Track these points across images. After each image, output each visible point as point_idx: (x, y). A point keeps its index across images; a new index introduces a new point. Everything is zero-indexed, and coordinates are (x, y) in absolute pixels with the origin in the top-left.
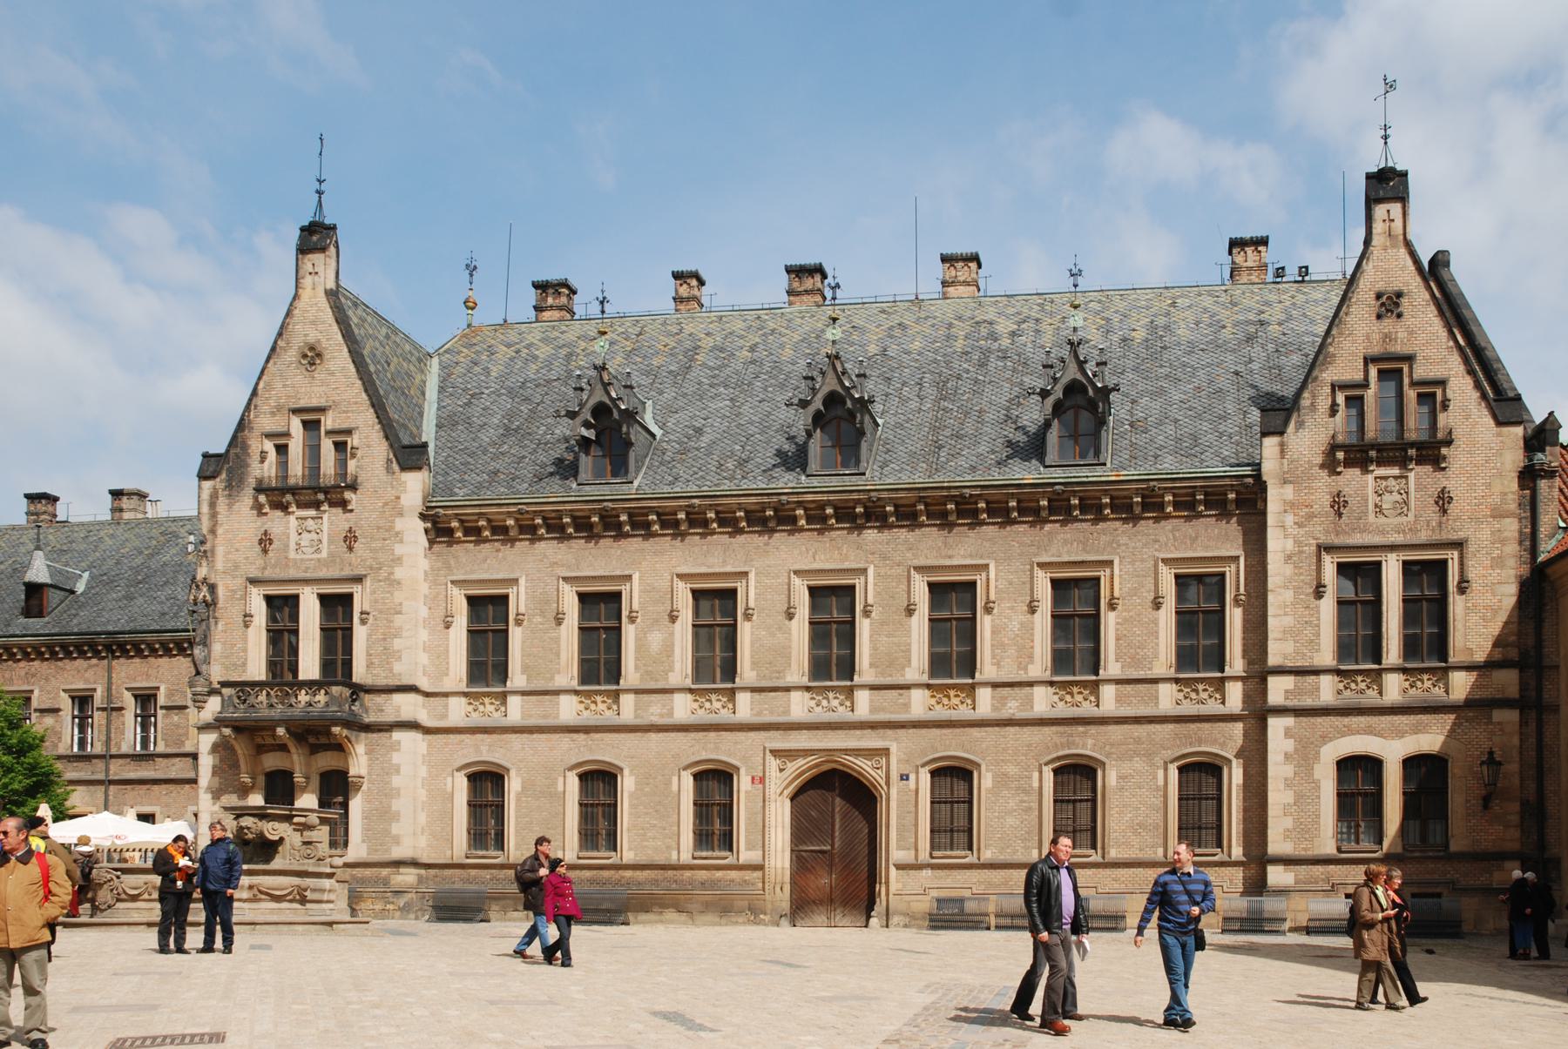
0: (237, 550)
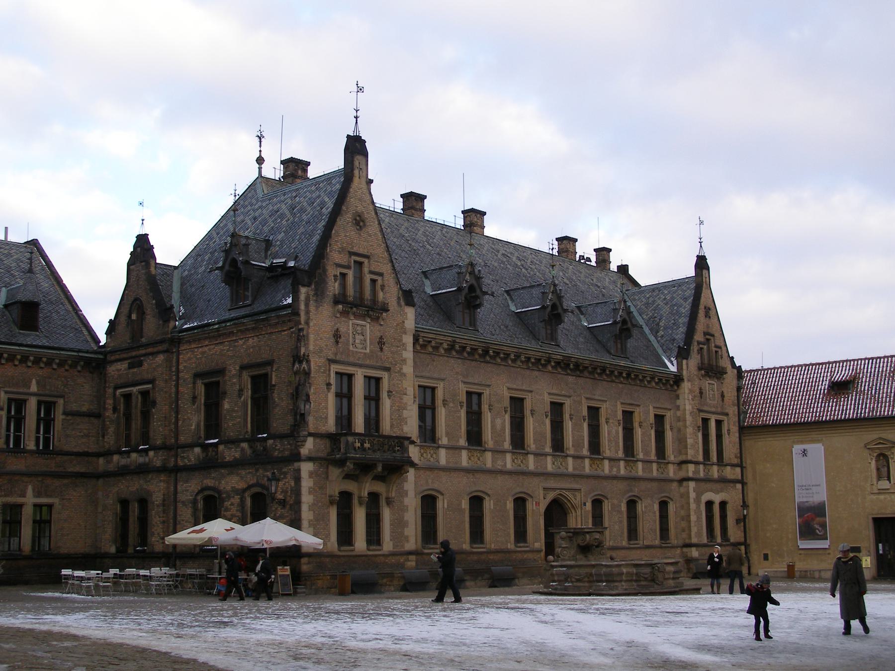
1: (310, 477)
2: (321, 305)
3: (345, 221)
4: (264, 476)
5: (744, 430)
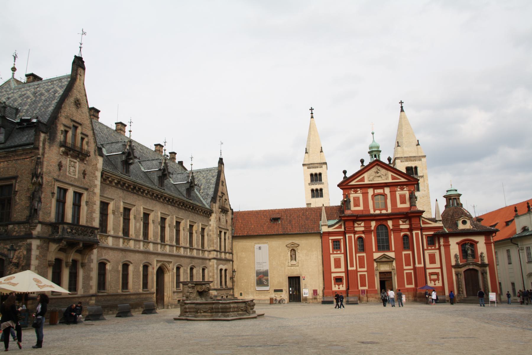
0: (51, 166)
1: (37, 249)
2: (52, 146)
3: (71, 100)
4: (4, 248)
5: (234, 237)
